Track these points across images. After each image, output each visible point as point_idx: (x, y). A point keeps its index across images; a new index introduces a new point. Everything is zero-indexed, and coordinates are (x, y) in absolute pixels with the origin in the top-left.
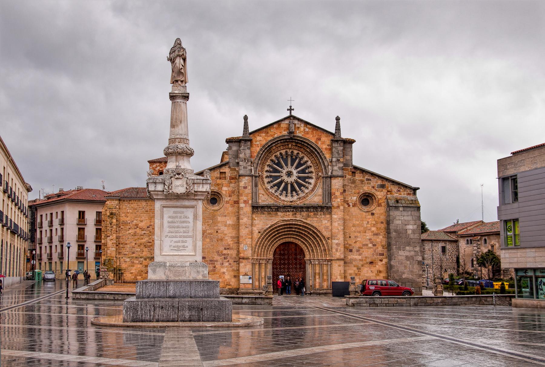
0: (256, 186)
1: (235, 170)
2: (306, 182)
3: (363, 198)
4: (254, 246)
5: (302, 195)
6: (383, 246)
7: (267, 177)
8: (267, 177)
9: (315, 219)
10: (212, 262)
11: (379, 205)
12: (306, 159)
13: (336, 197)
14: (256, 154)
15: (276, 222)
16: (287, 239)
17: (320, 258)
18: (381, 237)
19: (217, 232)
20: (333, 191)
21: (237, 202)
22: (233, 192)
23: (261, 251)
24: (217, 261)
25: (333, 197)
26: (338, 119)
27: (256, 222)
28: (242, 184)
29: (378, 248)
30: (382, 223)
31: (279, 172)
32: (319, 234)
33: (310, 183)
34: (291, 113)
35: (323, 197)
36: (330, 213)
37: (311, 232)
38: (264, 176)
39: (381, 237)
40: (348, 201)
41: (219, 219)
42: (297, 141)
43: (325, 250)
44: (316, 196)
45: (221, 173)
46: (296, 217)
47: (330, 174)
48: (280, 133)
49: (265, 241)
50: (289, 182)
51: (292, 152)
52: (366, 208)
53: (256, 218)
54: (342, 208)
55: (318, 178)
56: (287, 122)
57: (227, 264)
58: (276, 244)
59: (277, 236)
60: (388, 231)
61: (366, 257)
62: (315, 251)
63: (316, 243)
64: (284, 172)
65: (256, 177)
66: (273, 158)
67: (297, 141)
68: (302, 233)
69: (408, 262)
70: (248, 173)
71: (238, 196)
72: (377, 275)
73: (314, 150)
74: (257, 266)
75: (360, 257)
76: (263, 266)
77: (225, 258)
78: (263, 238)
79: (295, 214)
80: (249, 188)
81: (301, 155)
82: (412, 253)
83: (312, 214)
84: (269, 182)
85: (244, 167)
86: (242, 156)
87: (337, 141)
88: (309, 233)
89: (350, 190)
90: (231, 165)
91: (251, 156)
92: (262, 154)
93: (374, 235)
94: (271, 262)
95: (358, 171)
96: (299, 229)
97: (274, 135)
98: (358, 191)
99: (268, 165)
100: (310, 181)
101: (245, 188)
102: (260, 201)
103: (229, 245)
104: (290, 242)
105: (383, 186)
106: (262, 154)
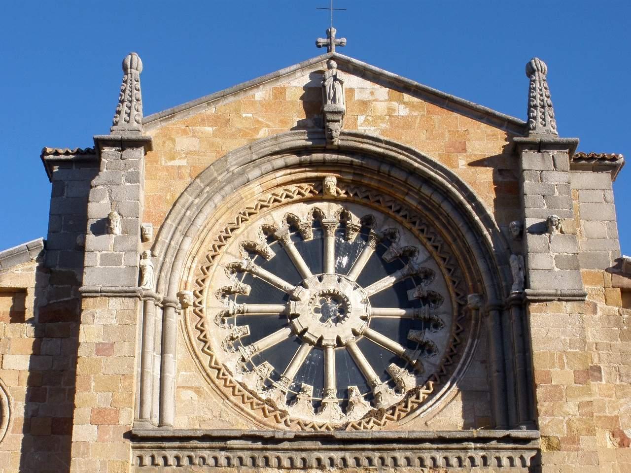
5: (389, 398)
13: (557, 395)
20: (539, 365)
25: (540, 393)
54: (586, 443)
55: (462, 317)
73: (436, 198)
85: (106, 259)
97: (256, 130)
101: (104, 349)
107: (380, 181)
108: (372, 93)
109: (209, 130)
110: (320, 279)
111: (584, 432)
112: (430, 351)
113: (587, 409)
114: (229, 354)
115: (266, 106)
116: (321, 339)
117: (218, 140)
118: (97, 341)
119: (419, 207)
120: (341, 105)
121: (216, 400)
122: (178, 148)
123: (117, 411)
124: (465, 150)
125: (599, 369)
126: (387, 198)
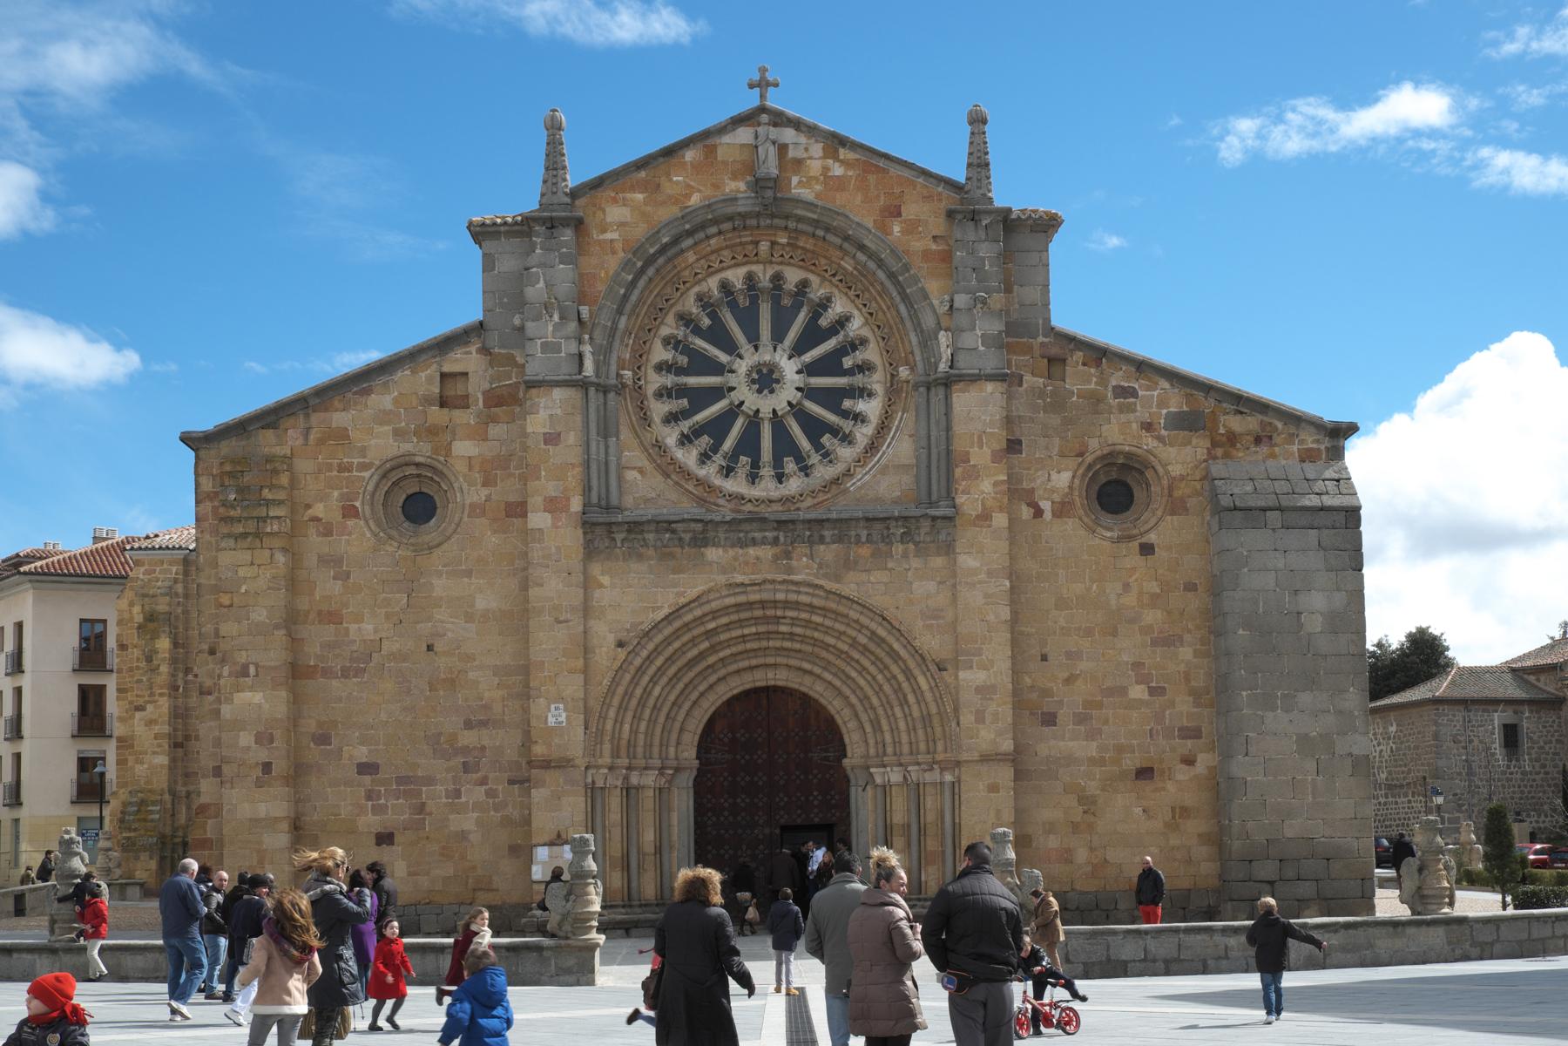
0: (607, 430)
1: (511, 360)
2: (845, 414)
3: (1103, 479)
4: (595, 705)
6: (1196, 694)
7: (663, 393)
8: (663, 393)
9: (878, 576)
10: (408, 783)
11: (1177, 507)
12: (839, 307)
13: (974, 474)
14: (601, 287)
15: (692, 593)
17: (905, 759)
18: (1186, 653)
19: (430, 648)
20: (958, 445)
21: (518, 510)
22: (503, 462)
23: (634, 732)
24: (430, 781)
25: (958, 472)
26: (978, 120)
27: (602, 597)
28: (538, 423)
29: (1172, 704)
30: (1190, 587)
31: (719, 369)
32: (896, 646)
33: (859, 418)
34: (762, 97)
35: (917, 476)
36: (949, 549)
37: (863, 640)
38: (651, 390)
39: (1186, 653)
40: (1032, 491)
41: (441, 586)
42: (792, 225)
44: (884, 471)
45: (443, 376)
46: (790, 570)
47: (943, 367)
48: (716, 186)
49: (653, 681)
50: (766, 412)
51: (777, 278)
53: (605, 580)
55: (894, 389)
56: (744, 135)
57: (479, 793)
58: (711, 697)
59: (711, 660)
60: (1215, 624)
61: (1120, 749)
62: (884, 722)
63: (887, 687)
64: (742, 367)
65: (604, 390)
66: (690, 305)
67: (792, 225)
68: (826, 647)
69: (1311, 765)
70: (566, 370)
71: (524, 479)
72: (1172, 826)
73: (872, 265)
74: (615, 802)
75: (1092, 749)
76: (648, 800)
77: (466, 768)
78: (640, 670)
79: (788, 555)
80: (572, 438)
81: (818, 291)
83: (865, 551)
84: (672, 418)
85: (546, 347)
86: (536, 291)
88: (854, 644)
89: (1042, 441)
90: (493, 339)
91: (581, 298)
92: (633, 283)
93: (1154, 643)
94: (687, 780)
95: (1079, 356)
97: (688, 196)
99: (666, 341)
100: (861, 406)
101: (552, 439)
102: (628, 501)
103: (487, 707)
104: (776, 689)
105: (1187, 422)
106: (633, 283)
108: (806, 149)
109: (640, 197)
110: (756, 347)
112: (863, 421)
114: (667, 430)
115: (697, 168)
116: (758, 411)
117: (649, 209)
120: (774, 172)
121: (660, 478)
122: (609, 219)
123: (568, 499)
124: (899, 215)
125: (1020, 442)
126: (823, 261)
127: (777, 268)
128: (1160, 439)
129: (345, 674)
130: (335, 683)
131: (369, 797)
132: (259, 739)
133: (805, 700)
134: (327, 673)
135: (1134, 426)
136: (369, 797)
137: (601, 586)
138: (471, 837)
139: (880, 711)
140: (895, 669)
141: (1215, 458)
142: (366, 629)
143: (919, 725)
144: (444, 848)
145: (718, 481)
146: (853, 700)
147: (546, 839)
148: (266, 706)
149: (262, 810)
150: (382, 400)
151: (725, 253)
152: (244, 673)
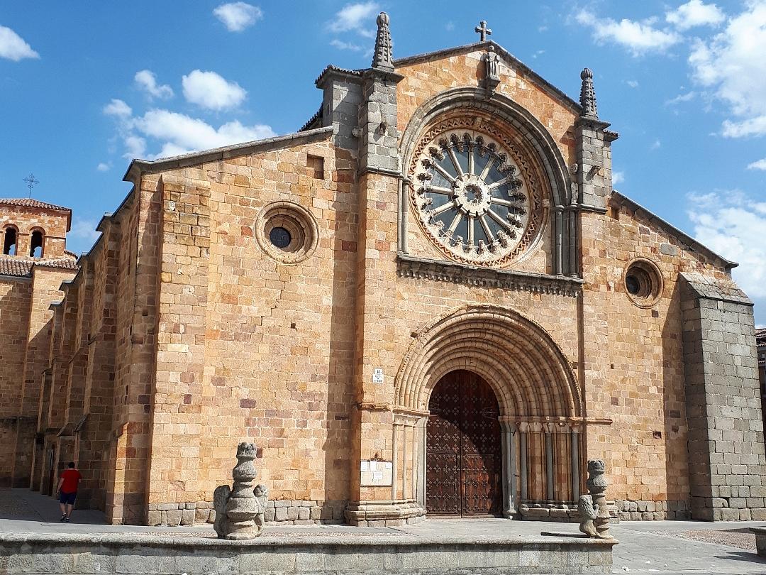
6: (676, 392)
9: (545, 312)
10: (273, 415)
12: (509, 162)
13: (591, 262)
15: (453, 309)
16: (462, 362)
19: (293, 326)
20: (585, 245)
25: (584, 259)
30: (674, 336)
37: (531, 347)
41: (302, 287)
42: (497, 111)
43: (564, 395)
47: (574, 202)
50: (473, 214)
51: (479, 139)
52: (639, 300)
55: (537, 212)
56: (477, 55)
61: (646, 420)
73: (535, 141)
75: (634, 420)
77: (311, 407)
80: (393, 207)
81: (500, 151)
82: (746, 413)
86: (374, 117)
87: (592, 125)
94: (423, 422)
96: (501, 335)
97: (451, 81)
98: (623, 255)
101: (381, 206)
104: (464, 370)
107: (503, 125)
109: (426, 76)
111: (602, 283)
113: (603, 271)
118: (376, 200)
119: (522, 144)
127: (480, 134)
128: (659, 257)
129: (237, 338)
130: (230, 342)
131: (248, 424)
132: (183, 378)
133: (478, 378)
134: (224, 336)
135: (649, 249)
136: (248, 424)
137: (403, 299)
138: (312, 454)
139: (530, 389)
140: (546, 366)
141: (682, 271)
142: (254, 309)
143: (558, 399)
144: (294, 461)
145: (448, 247)
146: (513, 382)
147: (369, 457)
148: (190, 355)
149: (182, 429)
150: (271, 161)
151: (458, 119)
152: (176, 330)
